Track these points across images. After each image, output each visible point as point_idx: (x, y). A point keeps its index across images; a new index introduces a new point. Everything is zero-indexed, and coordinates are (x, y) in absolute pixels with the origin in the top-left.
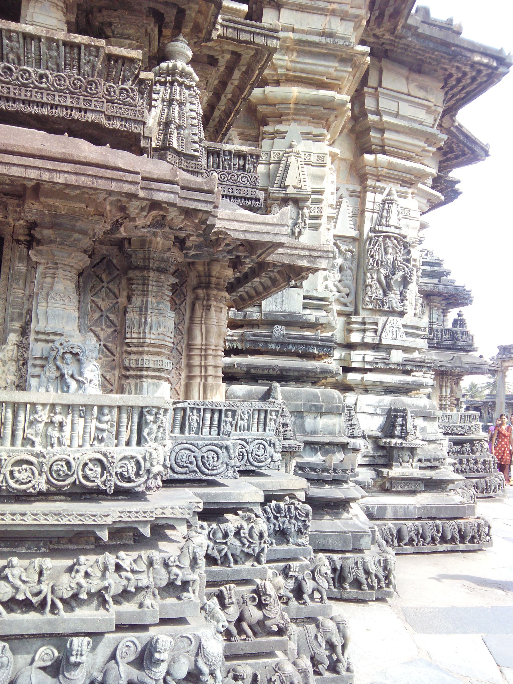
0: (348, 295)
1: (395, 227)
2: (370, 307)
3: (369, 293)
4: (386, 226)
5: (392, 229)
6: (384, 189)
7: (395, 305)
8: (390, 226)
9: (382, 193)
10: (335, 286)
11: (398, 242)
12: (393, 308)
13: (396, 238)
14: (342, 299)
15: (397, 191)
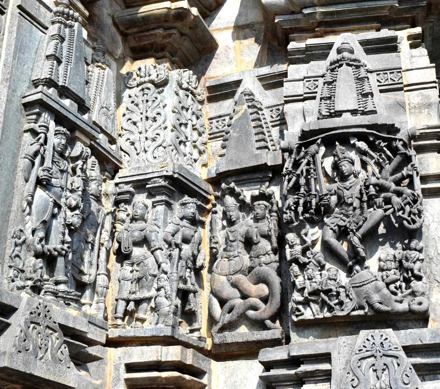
0: (265, 300)
1: (354, 112)
2: (308, 314)
3: (299, 281)
4: (331, 116)
5: (347, 119)
6: (330, 46)
7: (375, 298)
8: (339, 114)
9: (324, 56)
10: (234, 285)
11: (372, 145)
12: (371, 306)
13: (361, 137)
14: (251, 313)
15: (363, 43)
